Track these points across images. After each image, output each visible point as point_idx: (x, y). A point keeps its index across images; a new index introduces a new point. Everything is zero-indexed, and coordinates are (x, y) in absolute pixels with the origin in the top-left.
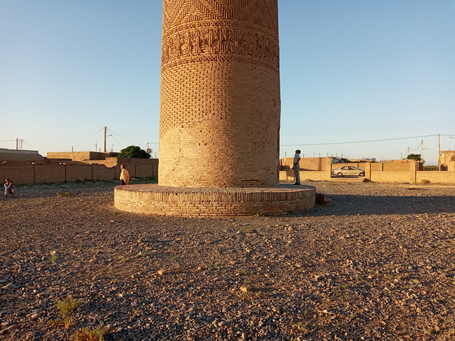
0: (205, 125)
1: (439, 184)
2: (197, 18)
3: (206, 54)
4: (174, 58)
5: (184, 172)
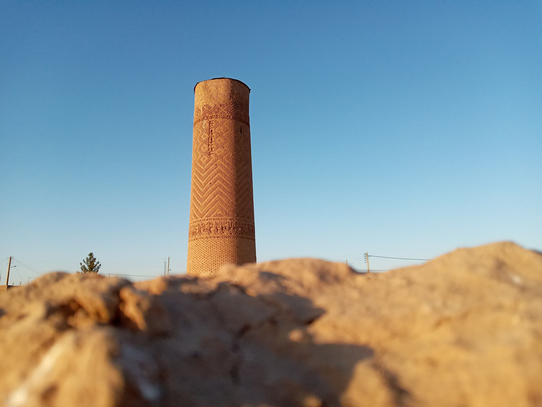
2: (220, 215)
3: (225, 234)
4: (204, 234)
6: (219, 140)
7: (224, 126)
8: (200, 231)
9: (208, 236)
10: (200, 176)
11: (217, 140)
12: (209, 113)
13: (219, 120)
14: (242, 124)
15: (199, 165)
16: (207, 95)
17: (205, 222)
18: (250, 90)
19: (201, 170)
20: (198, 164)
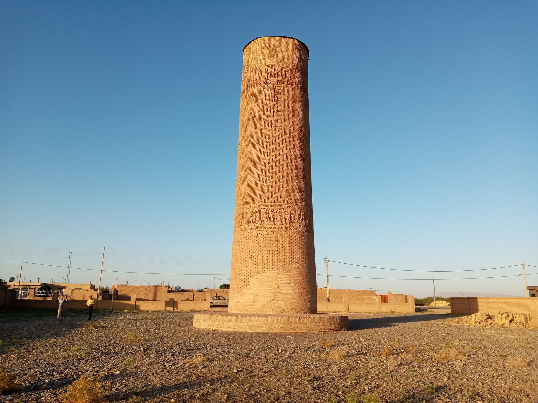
0: (295, 271)
2: (288, 202)
4: (269, 224)
5: (281, 303)
7: (289, 94)
12: (273, 76)
13: (287, 87)
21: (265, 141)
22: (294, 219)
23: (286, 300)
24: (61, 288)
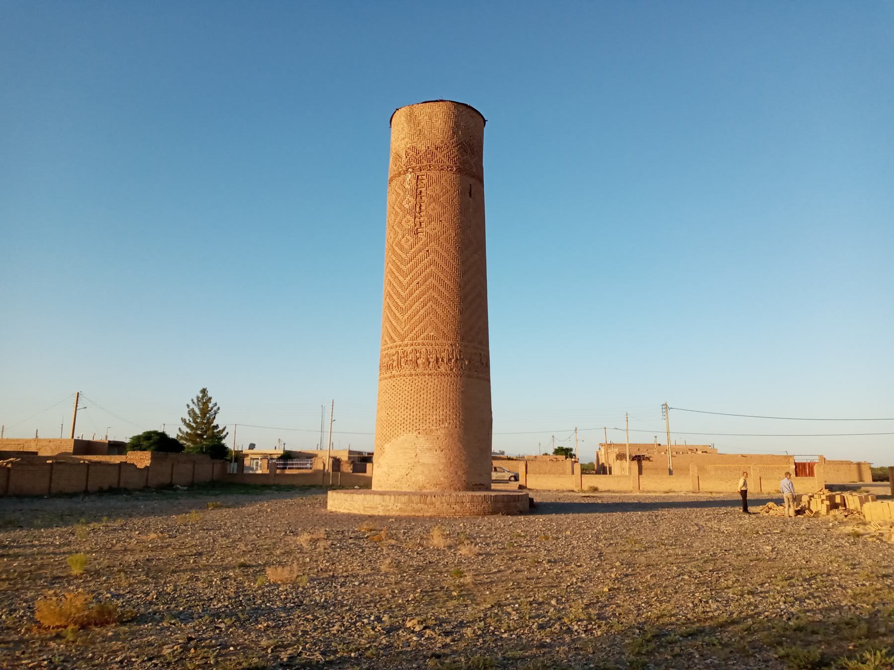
0: (441, 433)
1: (609, 491)
2: (433, 338)
3: (442, 369)
4: (407, 369)
6: (434, 209)
7: (441, 184)
8: (399, 363)
9: (413, 372)
10: (399, 269)
11: (430, 209)
12: (418, 162)
13: (434, 174)
14: (472, 181)
15: (399, 251)
16: (411, 131)
17: (409, 349)
18: (485, 121)
19: (402, 261)
20: (396, 249)
21: (404, 256)
22: (443, 360)
23: (426, 473)
24: (310, 456)
